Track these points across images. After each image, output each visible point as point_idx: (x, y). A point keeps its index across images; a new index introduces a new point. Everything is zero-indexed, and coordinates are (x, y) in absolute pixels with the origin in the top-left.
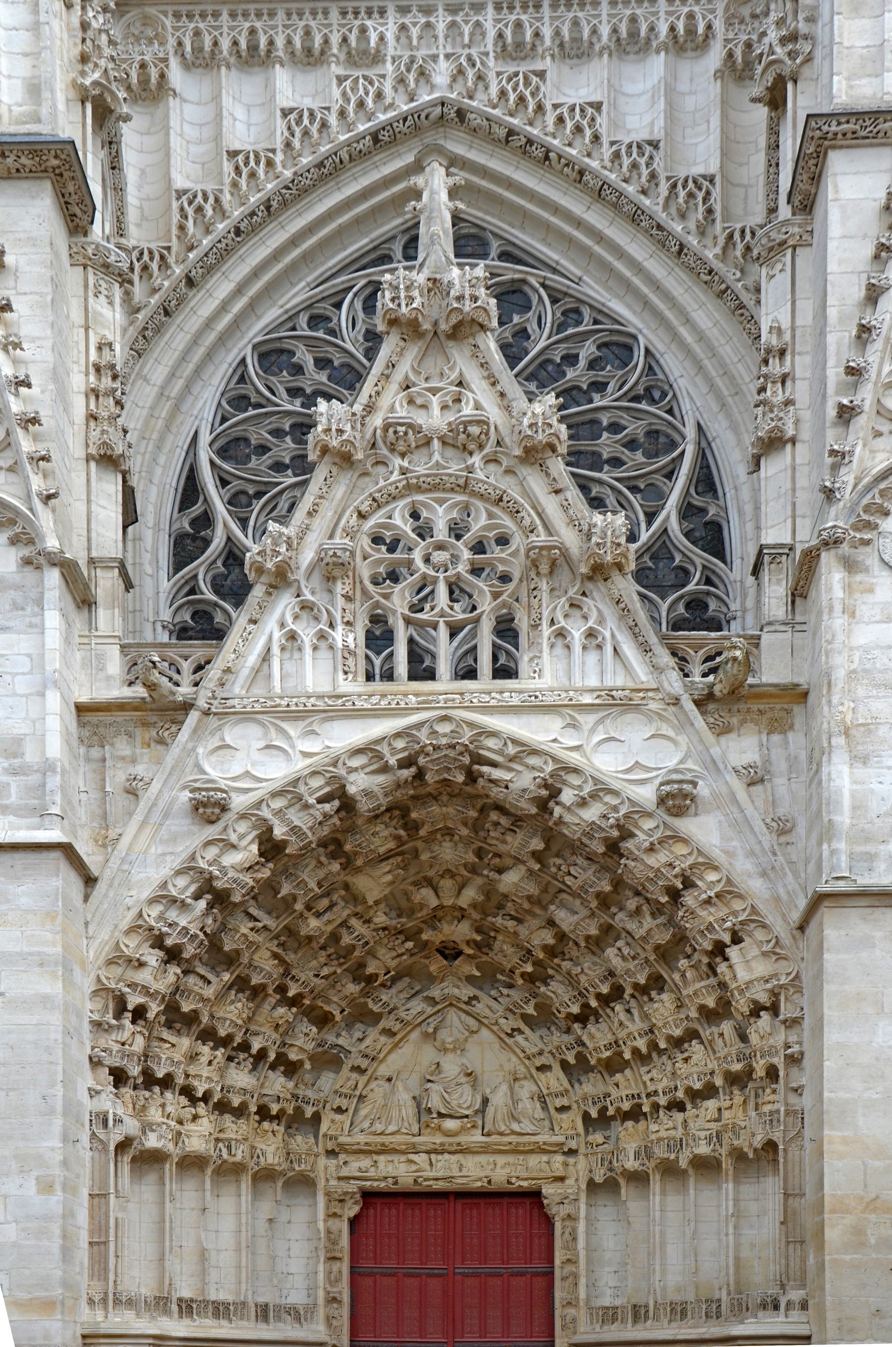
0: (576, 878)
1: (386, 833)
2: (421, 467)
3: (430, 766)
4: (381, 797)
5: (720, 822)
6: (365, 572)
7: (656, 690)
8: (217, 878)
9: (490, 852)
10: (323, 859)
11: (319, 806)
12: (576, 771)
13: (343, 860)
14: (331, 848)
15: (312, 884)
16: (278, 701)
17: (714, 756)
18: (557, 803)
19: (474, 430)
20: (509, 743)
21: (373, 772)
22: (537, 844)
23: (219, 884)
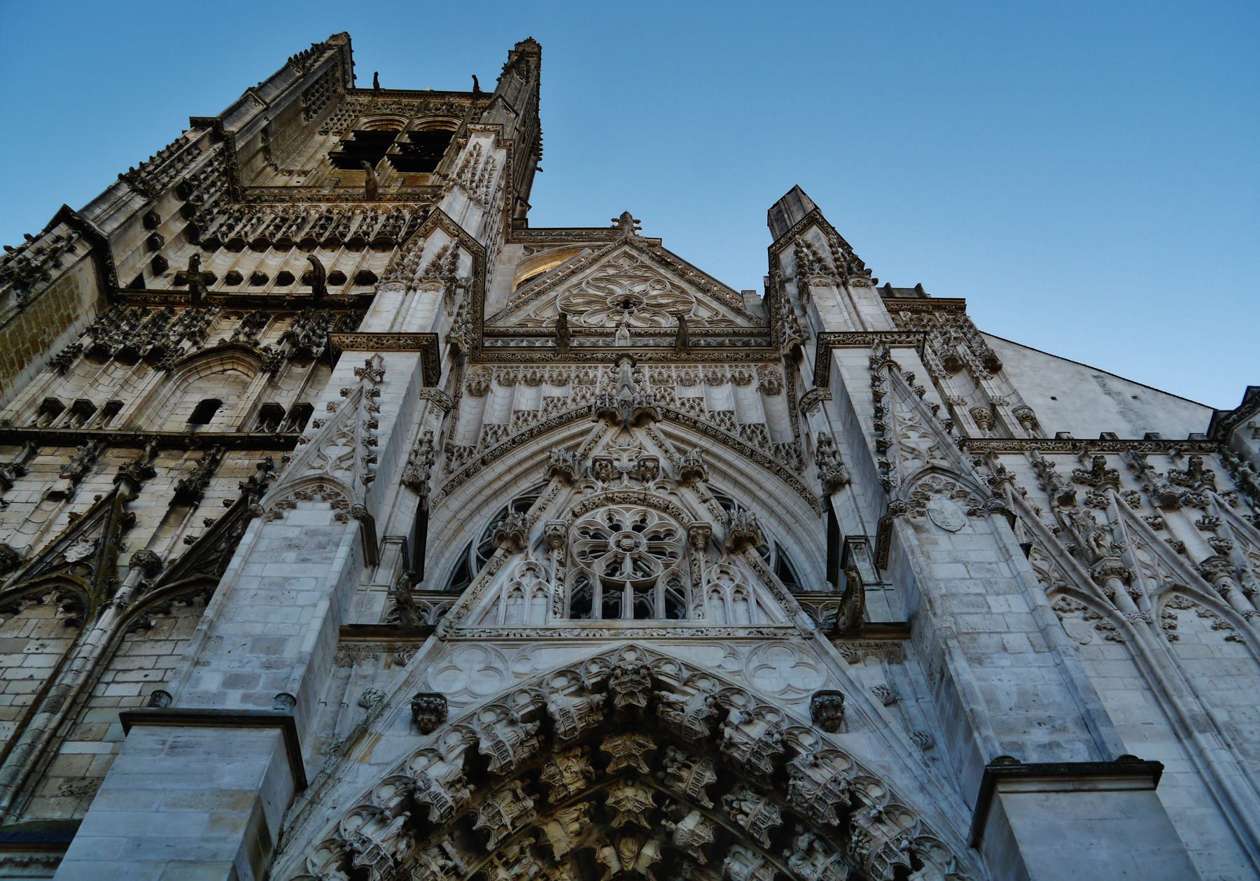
0: (747, 815)
1: (576, 768)
2: (615, 487)
3: (618, 689)
4: (576, 719)
5: (869, 738)
6: (576, 550)
7: (794, 627)
8: (420, 790)
9: (668, 797)
10: (519, 791)
11: (523, 725)
12: (740, 691)
13: (537, 796)
14: (528, 781)
15: (507, 820)
16: (500, 632)
17: (851, 677)
18: (726, 725)
19: (650, 464)
20: (683, 667)
21: (571, 694)
22: (710, 777)
23: (420, 796)
